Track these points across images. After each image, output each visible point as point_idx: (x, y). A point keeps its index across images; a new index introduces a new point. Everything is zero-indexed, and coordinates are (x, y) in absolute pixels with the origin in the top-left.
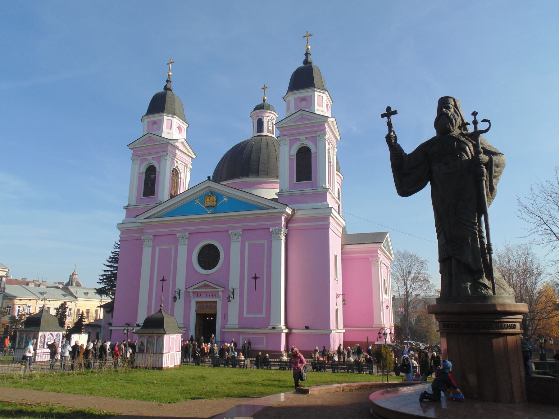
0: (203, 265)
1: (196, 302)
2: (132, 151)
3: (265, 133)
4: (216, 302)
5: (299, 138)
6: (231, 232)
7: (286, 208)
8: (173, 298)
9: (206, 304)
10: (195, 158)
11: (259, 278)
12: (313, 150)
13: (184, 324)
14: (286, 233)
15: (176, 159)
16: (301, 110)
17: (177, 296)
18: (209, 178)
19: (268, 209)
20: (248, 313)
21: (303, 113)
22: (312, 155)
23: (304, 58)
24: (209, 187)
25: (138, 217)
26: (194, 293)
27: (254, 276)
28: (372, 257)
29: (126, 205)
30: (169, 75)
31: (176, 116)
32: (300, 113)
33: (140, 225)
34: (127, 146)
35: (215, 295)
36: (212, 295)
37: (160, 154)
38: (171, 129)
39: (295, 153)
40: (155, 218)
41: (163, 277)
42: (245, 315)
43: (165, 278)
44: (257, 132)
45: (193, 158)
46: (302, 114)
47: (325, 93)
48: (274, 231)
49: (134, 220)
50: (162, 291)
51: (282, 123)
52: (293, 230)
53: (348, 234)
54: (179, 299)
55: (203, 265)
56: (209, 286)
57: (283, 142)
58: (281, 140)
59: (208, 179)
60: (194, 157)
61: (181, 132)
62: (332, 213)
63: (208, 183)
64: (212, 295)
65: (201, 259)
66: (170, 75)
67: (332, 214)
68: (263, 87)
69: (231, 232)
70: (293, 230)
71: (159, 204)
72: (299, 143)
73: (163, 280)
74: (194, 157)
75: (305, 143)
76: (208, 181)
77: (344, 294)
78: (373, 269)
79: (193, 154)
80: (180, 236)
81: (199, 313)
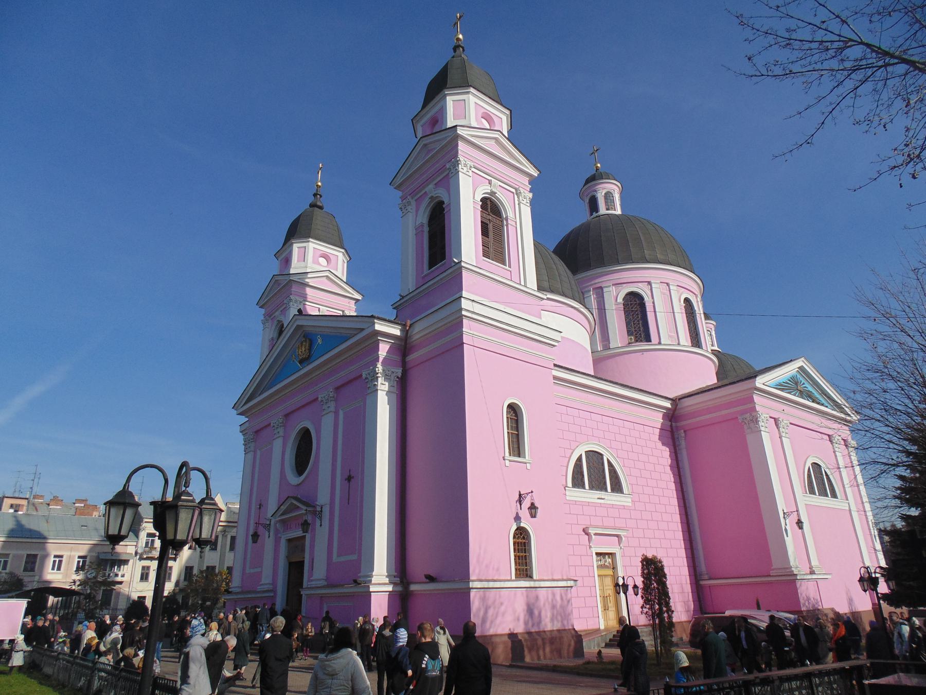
5: (426, 192)
6: (322, 398)
7: (374, 324)
10: (361, 299)
13: (272, 584)
14: (398, 377)
15: (307, 303)
20: (339, 555)
21: (424, 142)
28: (744, 412)
30: (317, 185)
31: (311, 240)
38: (304, 261)
42: (335, 558)
45: (357, 300)
46: (425, 145)
47: (469, 92)
48: (368, 376)
53: (716, 382)
60: (359, 297)
61: (331, 263)
62: (461, 309)
66: (320, 187)
67: (464, 313)
69: (322, 398)
72: (428, 199)
74: (359, 297)
77: (532, 492)
78: (750, 438)
79: (353, 292)
81: (294, 560)
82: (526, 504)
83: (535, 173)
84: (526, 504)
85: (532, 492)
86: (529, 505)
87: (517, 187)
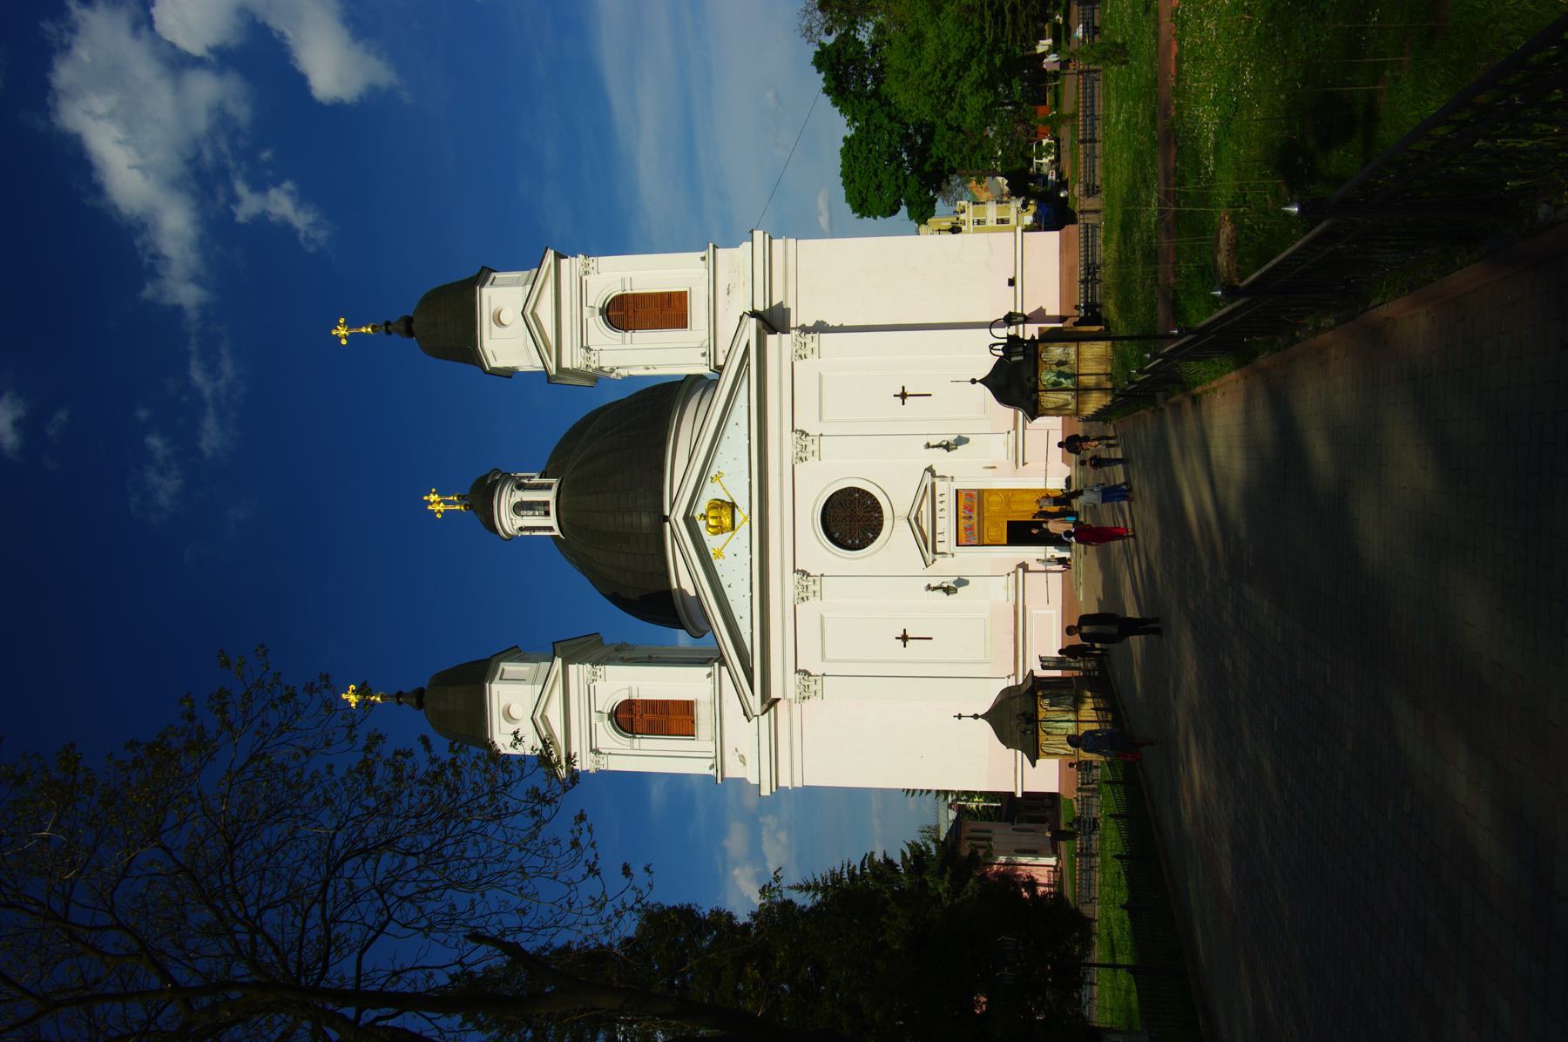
0: (871, 536)
1: (957, 545)
3: (549, 496)
4: (957, 490)
8: (948, 594)
9: (962, 521)
11: (903, 387)
19: (748, 365)
22: (629, 292)
26: (935, 552)
27: (899, 400)
35: (941, 495)
36: (941, 502)
37: (589, 686)
43: (900, 634)
44: (547, 514)
50: (931, 639)
55: (871, 536)
64: (941, 502)
65: (857, 542)
75: (601, 306)
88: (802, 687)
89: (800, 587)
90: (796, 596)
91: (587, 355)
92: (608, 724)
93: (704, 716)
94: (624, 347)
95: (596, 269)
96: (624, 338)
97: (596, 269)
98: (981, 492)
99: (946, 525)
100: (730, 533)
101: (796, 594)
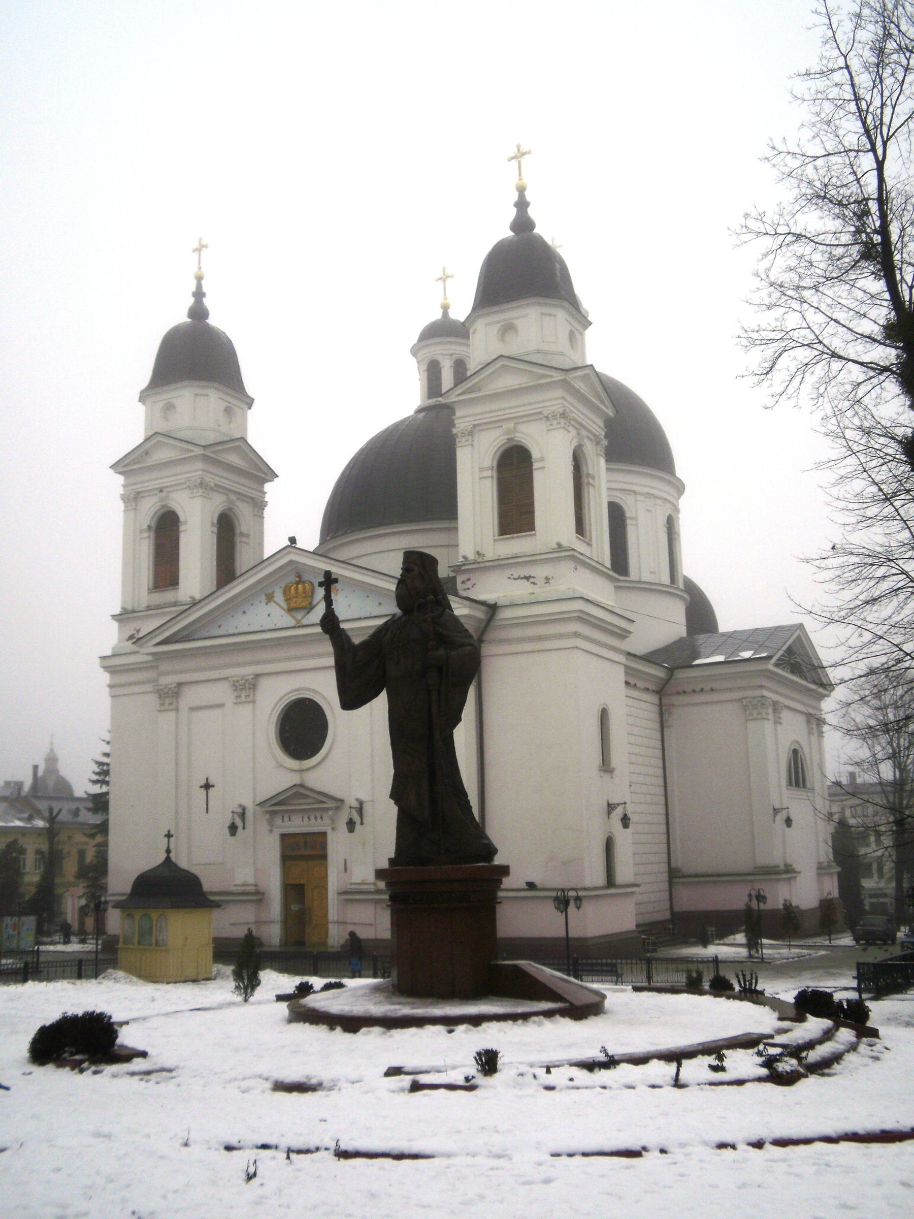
0: (292, 748)
2: (121, 479)
12: (535, 454)
16: (501, 356)
17: (239, 822)
18: (293, 540)
23: (512, 213)
24: (291, 562)
25: (141, 642)
29: (118, 611)
32: (502, 363)
33: (150, 658)
34: (111, 467)
35: (321, 818)
36: (316, 818)
39: (495, 464)
40: (177, 642)
41: (207, 779)
46: (503, 366)
49: (135, 648)
51: (457, 393)
52: (493, 656)
54: (244, 828)
55: (292, 748)
56: (307, 797)
57: (463, 439)
58: (459, 434)
59: (289, 544)
63: (290, 552)
65: (287, 735)
68: (441, 274)
70: (493, 656)
71: (189, 606)
73: (207, 786)
75: (516, 439)
76: (290, 549)
80: (236, 683)
82: (618, 813)
83: (611, 413)
84: (618, 813)
85: (625, 803)
86: (621, 816)
87: (597, 433)
88: (167, 690)
89: (243, 682)
90: (235, 679)
91: (466, 433)
92: (157, 506)
93: (168, 596)
94: (477, 470)
95: (551, 428)
96: (487, 469)
97: (551, 428)
98: (324, 857)
99: (298, 825)
100: (285, 607)
101: (238, 679)
